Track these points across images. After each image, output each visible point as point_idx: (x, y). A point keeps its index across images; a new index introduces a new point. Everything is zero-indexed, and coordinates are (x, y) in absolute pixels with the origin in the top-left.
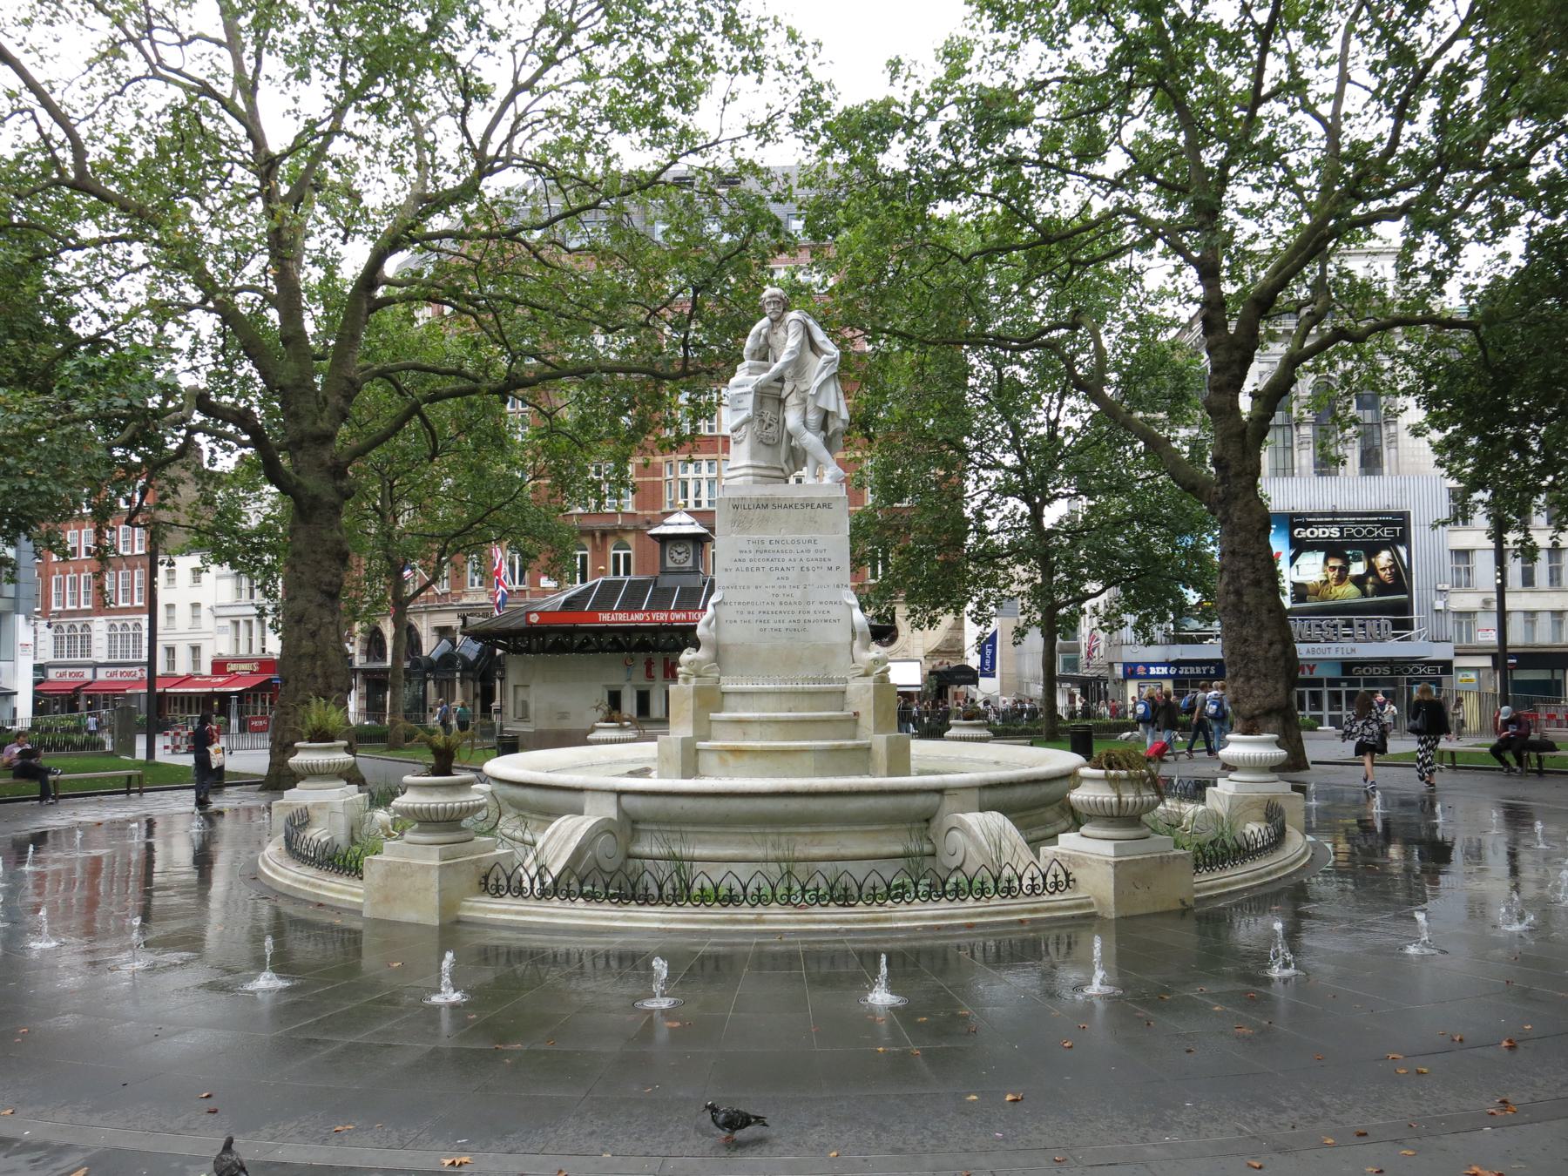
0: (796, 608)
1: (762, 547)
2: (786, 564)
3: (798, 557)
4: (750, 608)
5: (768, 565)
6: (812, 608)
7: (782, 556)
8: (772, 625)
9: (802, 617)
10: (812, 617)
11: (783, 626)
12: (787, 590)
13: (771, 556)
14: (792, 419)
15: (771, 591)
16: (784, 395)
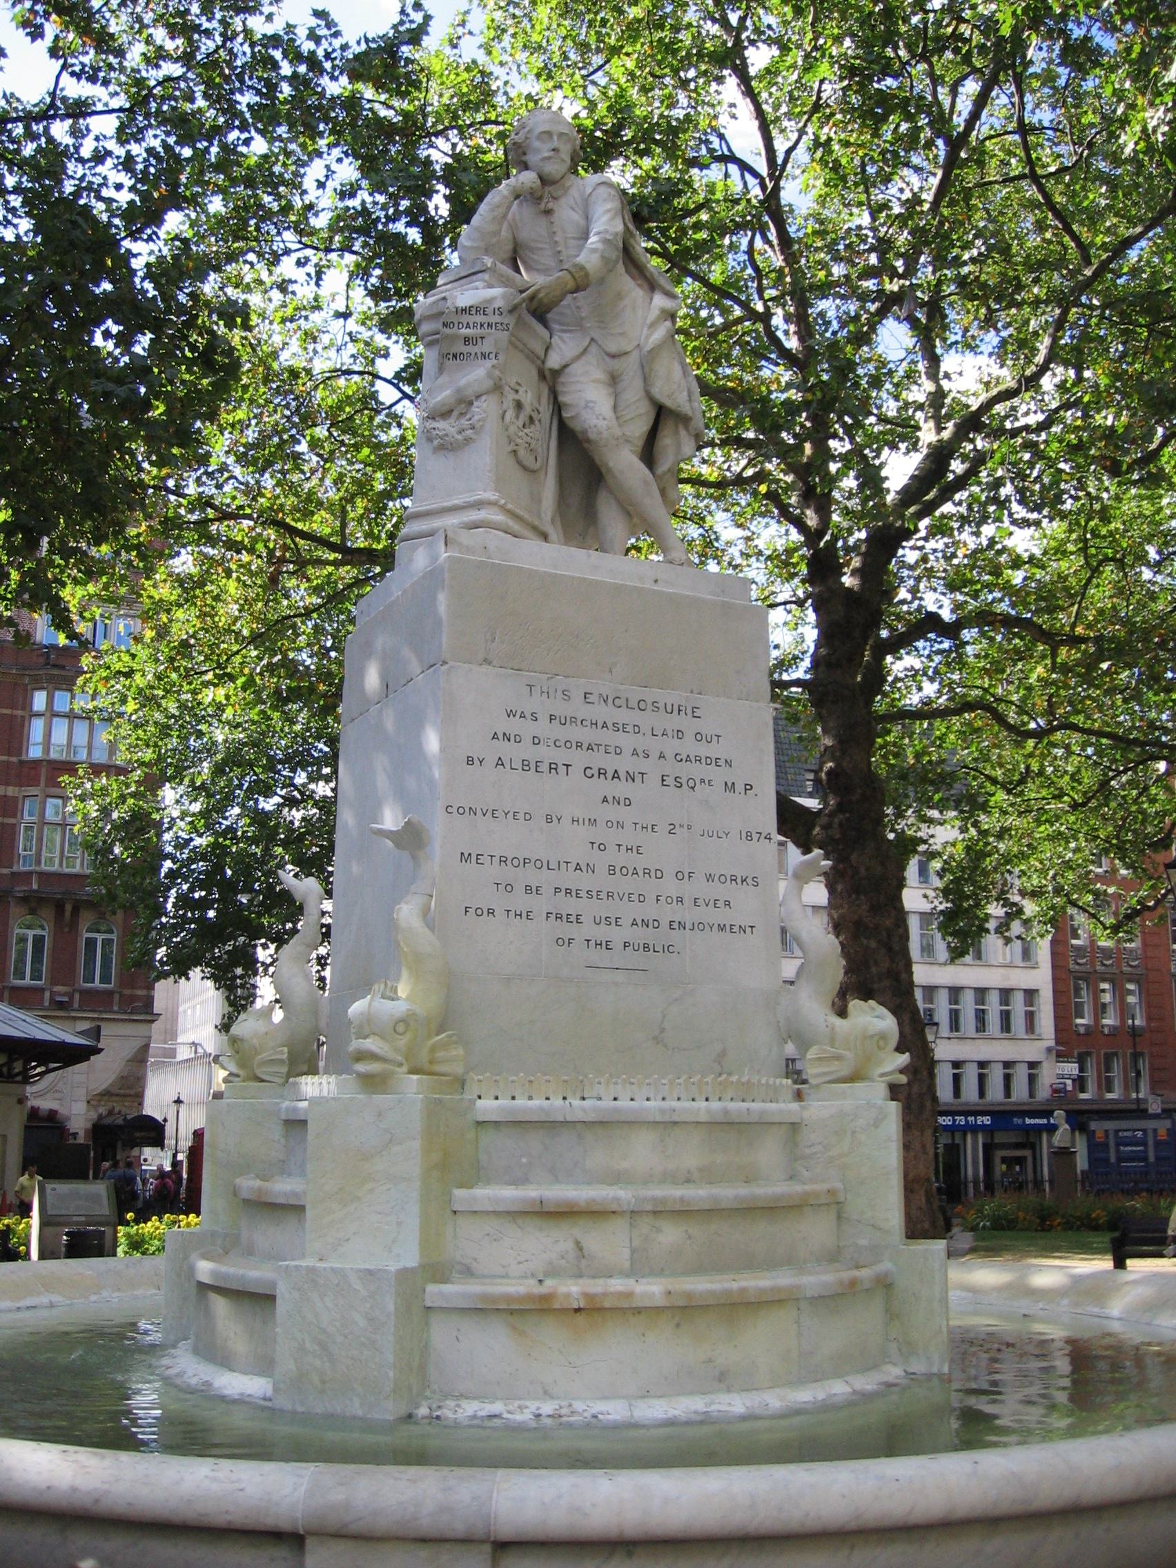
0: (650, 887)
1: (560, 708)
2: (625, 764)
3: (655, 745)
4: (531, 876)
5: (579, 759)
7: (621, 739)
8: (588, 930)
9: (667, 913)
10: (687, 914)
12: (629, 837)
15: (583, 831)
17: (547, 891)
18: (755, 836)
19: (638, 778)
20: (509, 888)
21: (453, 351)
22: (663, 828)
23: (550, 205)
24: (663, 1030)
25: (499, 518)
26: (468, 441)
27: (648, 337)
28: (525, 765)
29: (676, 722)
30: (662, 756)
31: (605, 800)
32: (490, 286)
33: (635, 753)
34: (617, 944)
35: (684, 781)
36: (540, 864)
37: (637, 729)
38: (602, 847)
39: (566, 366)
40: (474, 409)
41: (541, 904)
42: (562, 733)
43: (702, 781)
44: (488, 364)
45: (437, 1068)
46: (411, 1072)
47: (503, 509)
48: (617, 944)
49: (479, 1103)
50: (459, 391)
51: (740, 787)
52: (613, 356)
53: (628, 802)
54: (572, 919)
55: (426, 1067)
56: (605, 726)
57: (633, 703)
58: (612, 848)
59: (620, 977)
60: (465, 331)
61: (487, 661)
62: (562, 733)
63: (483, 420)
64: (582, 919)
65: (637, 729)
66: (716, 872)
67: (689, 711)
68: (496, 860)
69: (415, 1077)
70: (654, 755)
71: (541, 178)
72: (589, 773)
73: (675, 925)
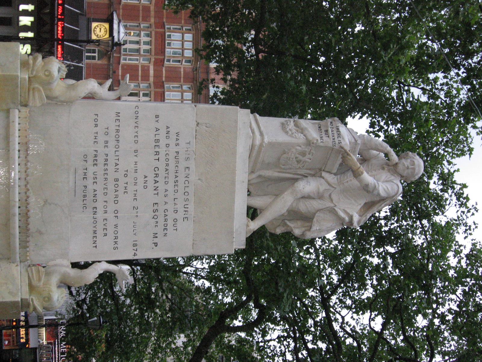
1: (182, 157)
2: (161, 186)
4: (112, 143)
5: (162, 165)
6: (110, 216)
8: (91, 169)
9: (100, 205)
10: (100, 215)
11: (90, 181)
12: (131, 188)
13: (172, 168)
14: (308, 186)
16: (324, 174)
17: (106, 150)
18: (135, 248)
19: (156, 192)
20: (107, 134)
21: (322, 128)
22: (135, 204)
23: (386, 169)
24: (50, 204)
25: (258, 142)
26: (287, 133)
27: (340, 209)
28: (157, 141)
29: (181, 210)
30: (166, 203)
31: (146, 177)
32: (350, 143)
33: (166, 191)
34: (85, 183)
35: (156, 213)
36: (117, 147)
37: (176, 191)
38: (126, 175)
39: (323, 178)
40: (300, 134)
41: (100, 148)
42: (171, 157)
43: (157, 222)
44: (319, 139)
45: (31, 92)
46: (29, 78)
47: (261, 145)
48: (85, 183)
49: (17, 111)
50: (306, 128)
51: (156, 240)
52: (330, 196)
53: (145, 187)
54: (95, 162)
55: (32, 87)
56: (176, 177)
57: (187, 189)
58: (126, 179)
59: (71, 184)
60: (330, 130)
61: (198, 124)
62: (171, 157)
63: (296, 138)
64: (95, 166)
65: (176, 191)
66: (119, 228)
67: (186, 216)
68: (117, 128)
69: (27, 77)
70: (166, 199)
71: (397, 164)
72: (156, 169)
73: (95, 210)
